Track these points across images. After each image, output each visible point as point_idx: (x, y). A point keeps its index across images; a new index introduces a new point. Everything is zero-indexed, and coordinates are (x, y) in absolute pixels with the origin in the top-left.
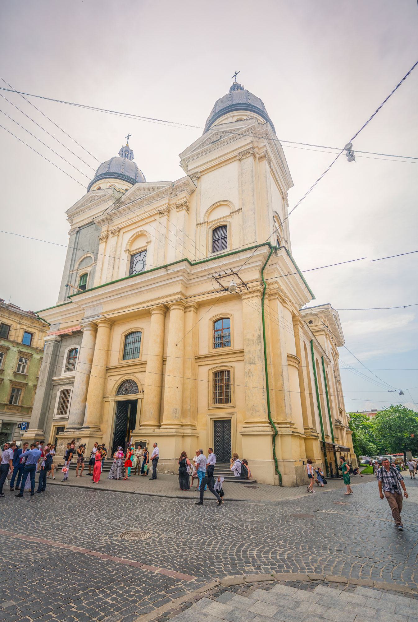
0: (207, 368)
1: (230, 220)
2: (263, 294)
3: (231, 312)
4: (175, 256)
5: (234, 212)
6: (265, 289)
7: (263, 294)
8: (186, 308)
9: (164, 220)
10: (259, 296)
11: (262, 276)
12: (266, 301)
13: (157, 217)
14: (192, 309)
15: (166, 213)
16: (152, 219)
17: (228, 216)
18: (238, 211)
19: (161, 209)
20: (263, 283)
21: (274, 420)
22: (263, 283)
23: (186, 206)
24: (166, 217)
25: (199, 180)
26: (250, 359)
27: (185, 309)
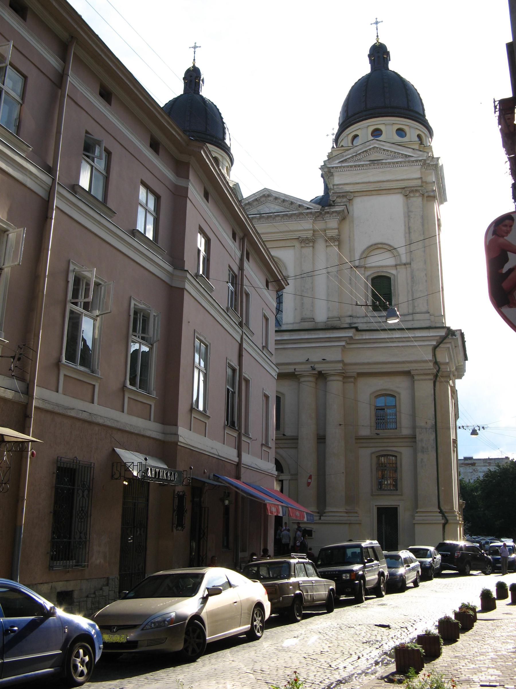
0: (369, 451)
1: (394, 272)
2: (436, 376)
3: (398, 390)
4: (328, 308)
5: (399, 265)
6: (438, 371)
7: (436, 376)
8: (344, 377)
9: (308, 251)
10: (431, 379)
11: (434, 355)
12: (437, 384)
13: (297, 244)
14: (352, 380)
15: (311, 244)
16: (289, 243)
17: (391, 266)
18: (405, 264)
19: (304, 235)
20: (436, 363)
21: (444, 510)
22: (436, 363)
23: (337, 240)
24: (311, 248)
25: (351, 201)
26: (423, 447)
27: (343, 379)
